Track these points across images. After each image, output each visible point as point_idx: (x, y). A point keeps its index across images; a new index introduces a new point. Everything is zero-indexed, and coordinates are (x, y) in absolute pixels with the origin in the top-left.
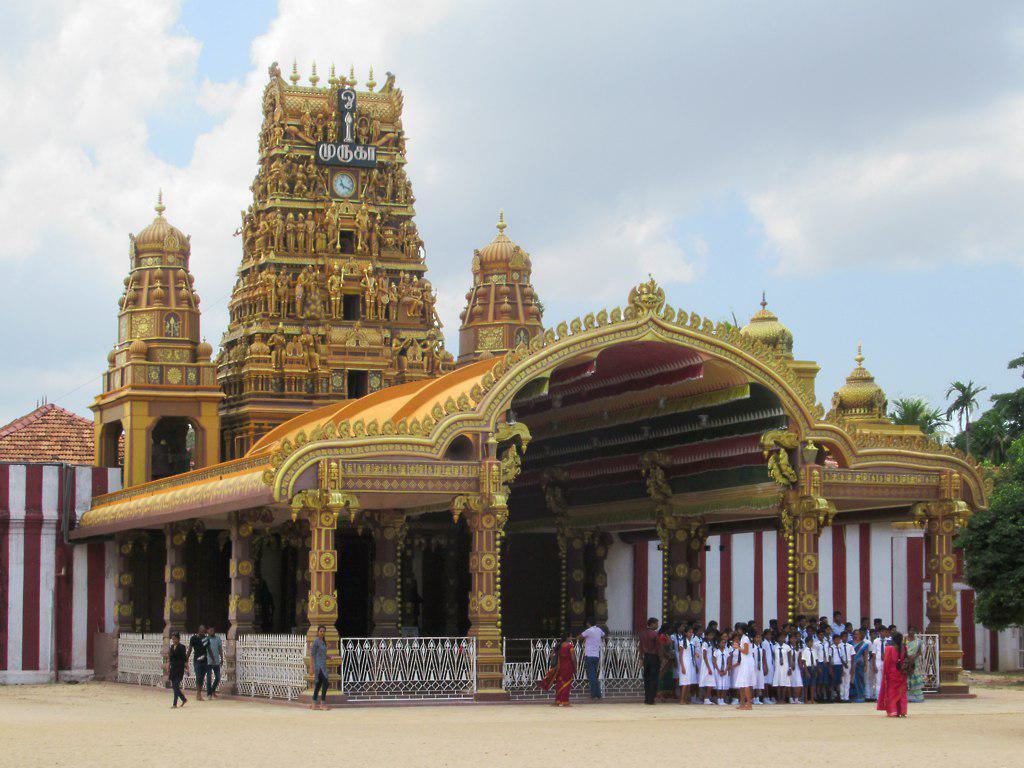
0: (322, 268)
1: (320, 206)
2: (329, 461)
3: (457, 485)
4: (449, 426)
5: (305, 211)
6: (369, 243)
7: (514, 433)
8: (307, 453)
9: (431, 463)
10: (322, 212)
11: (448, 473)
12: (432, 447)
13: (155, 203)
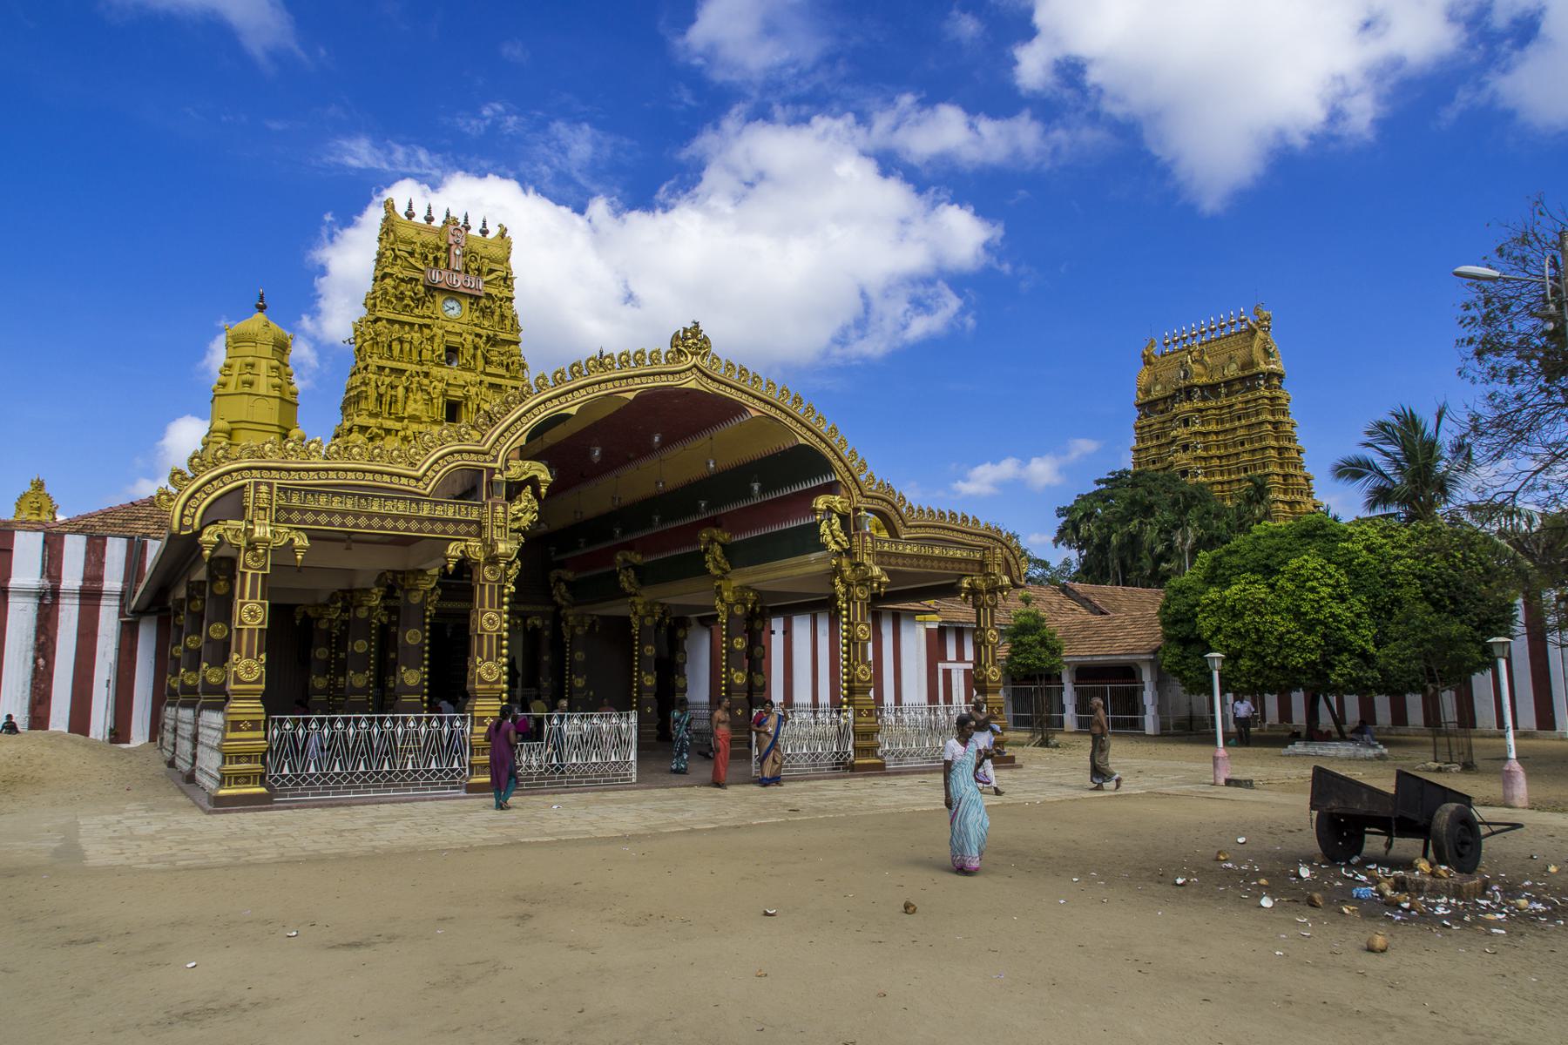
0: (427, 375)
1: (427, 321)
2: (257, 484)
3: (451, 528)
4: (442, 457)
5: (412, 325)
6: (474, 357)
7: (531, 474)
8: (229, 473)
9: (417, 499)
10: (428, 326)
11: (439, 512)
12: (418, 479)
13: (257, 301)
